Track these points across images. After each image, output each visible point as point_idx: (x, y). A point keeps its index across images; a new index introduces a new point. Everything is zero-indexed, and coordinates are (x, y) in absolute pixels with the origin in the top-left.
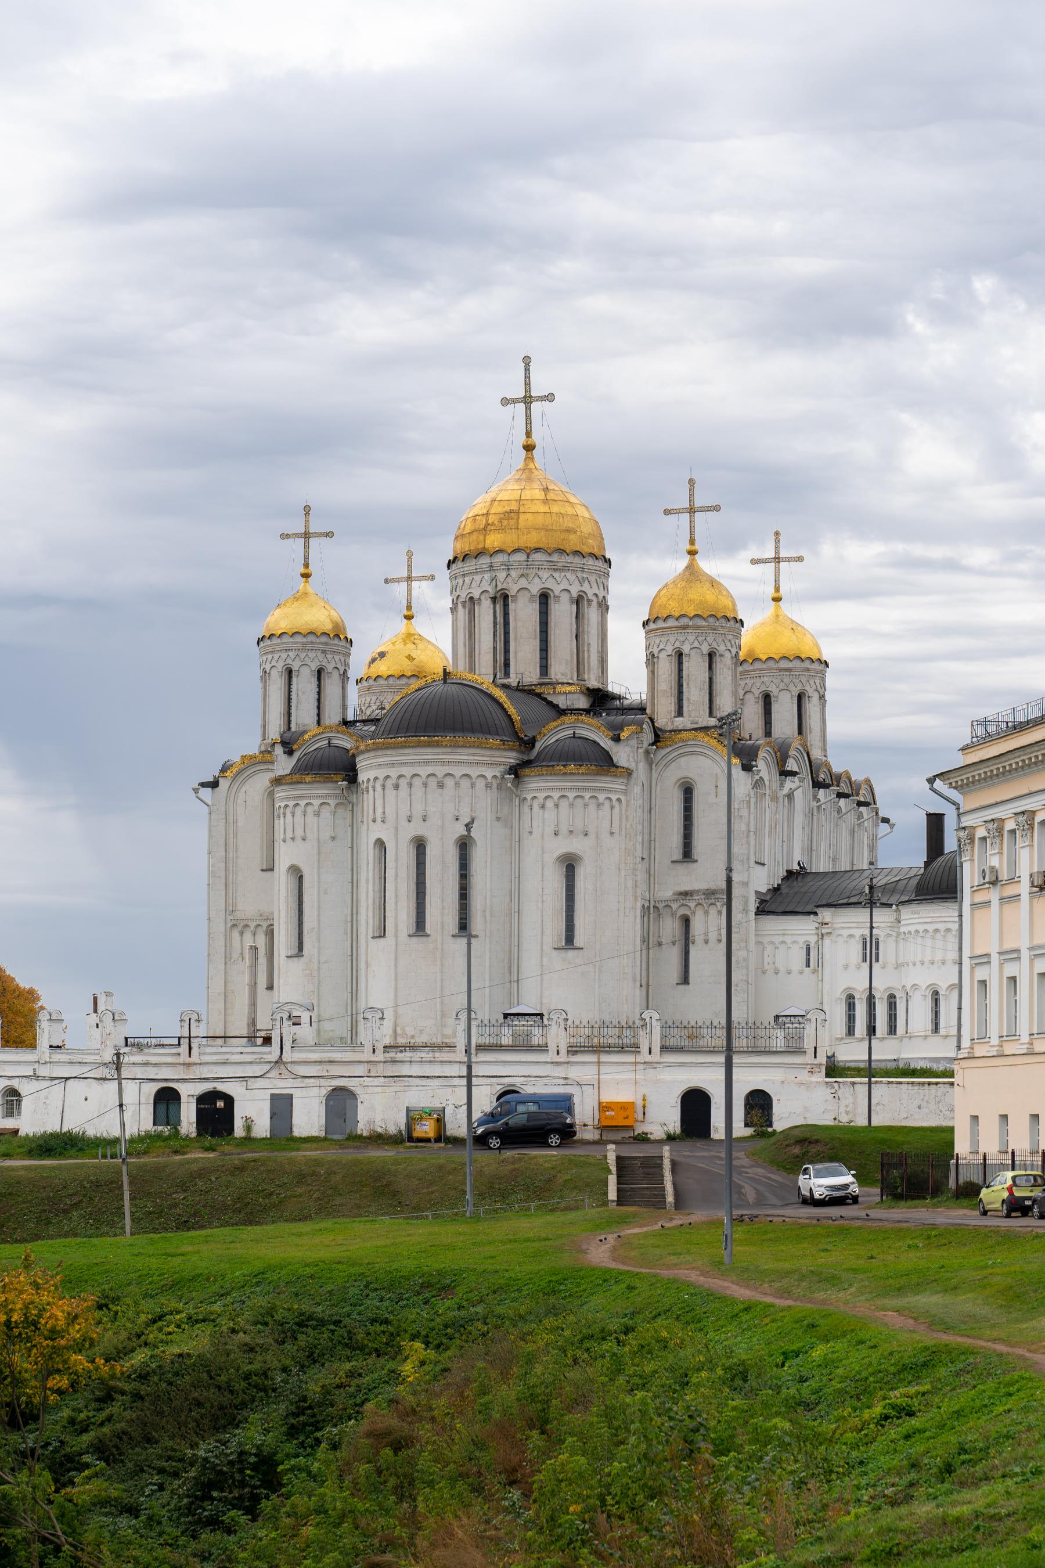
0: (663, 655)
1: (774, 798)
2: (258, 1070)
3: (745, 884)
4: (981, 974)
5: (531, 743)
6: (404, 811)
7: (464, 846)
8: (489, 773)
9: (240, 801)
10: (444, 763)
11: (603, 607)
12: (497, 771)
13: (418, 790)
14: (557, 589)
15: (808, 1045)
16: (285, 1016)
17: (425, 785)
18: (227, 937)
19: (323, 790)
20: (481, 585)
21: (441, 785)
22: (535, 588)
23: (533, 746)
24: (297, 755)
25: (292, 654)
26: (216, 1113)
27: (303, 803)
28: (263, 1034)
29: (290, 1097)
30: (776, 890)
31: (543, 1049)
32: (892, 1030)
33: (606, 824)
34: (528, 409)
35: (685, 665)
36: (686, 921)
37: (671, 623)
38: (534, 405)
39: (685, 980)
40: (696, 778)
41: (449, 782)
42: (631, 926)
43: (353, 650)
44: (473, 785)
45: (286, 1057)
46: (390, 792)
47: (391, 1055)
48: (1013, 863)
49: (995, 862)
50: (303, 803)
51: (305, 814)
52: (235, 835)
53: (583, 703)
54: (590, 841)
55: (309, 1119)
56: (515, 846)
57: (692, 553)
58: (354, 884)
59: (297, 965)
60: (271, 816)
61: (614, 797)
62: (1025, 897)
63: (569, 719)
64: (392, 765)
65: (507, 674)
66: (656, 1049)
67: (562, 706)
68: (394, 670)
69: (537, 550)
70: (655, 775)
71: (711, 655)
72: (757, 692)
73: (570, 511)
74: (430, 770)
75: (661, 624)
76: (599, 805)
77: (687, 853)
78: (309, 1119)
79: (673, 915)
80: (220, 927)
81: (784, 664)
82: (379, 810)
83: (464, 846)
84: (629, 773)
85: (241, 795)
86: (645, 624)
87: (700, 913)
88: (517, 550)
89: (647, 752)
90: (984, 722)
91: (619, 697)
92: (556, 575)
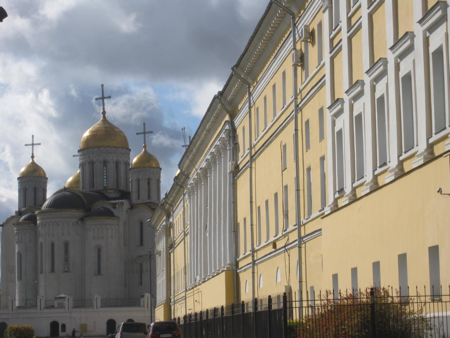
7: (66, 245)
21: (58, 224)
34: (103, 101)
35: (140, 183)
36: (141, 265)
38: (106, 101)
39: (141, 284)
69: (102, 147)
71: (149, 180)
77: (142, 243)
83: (66, 245)
89: (127, 211)
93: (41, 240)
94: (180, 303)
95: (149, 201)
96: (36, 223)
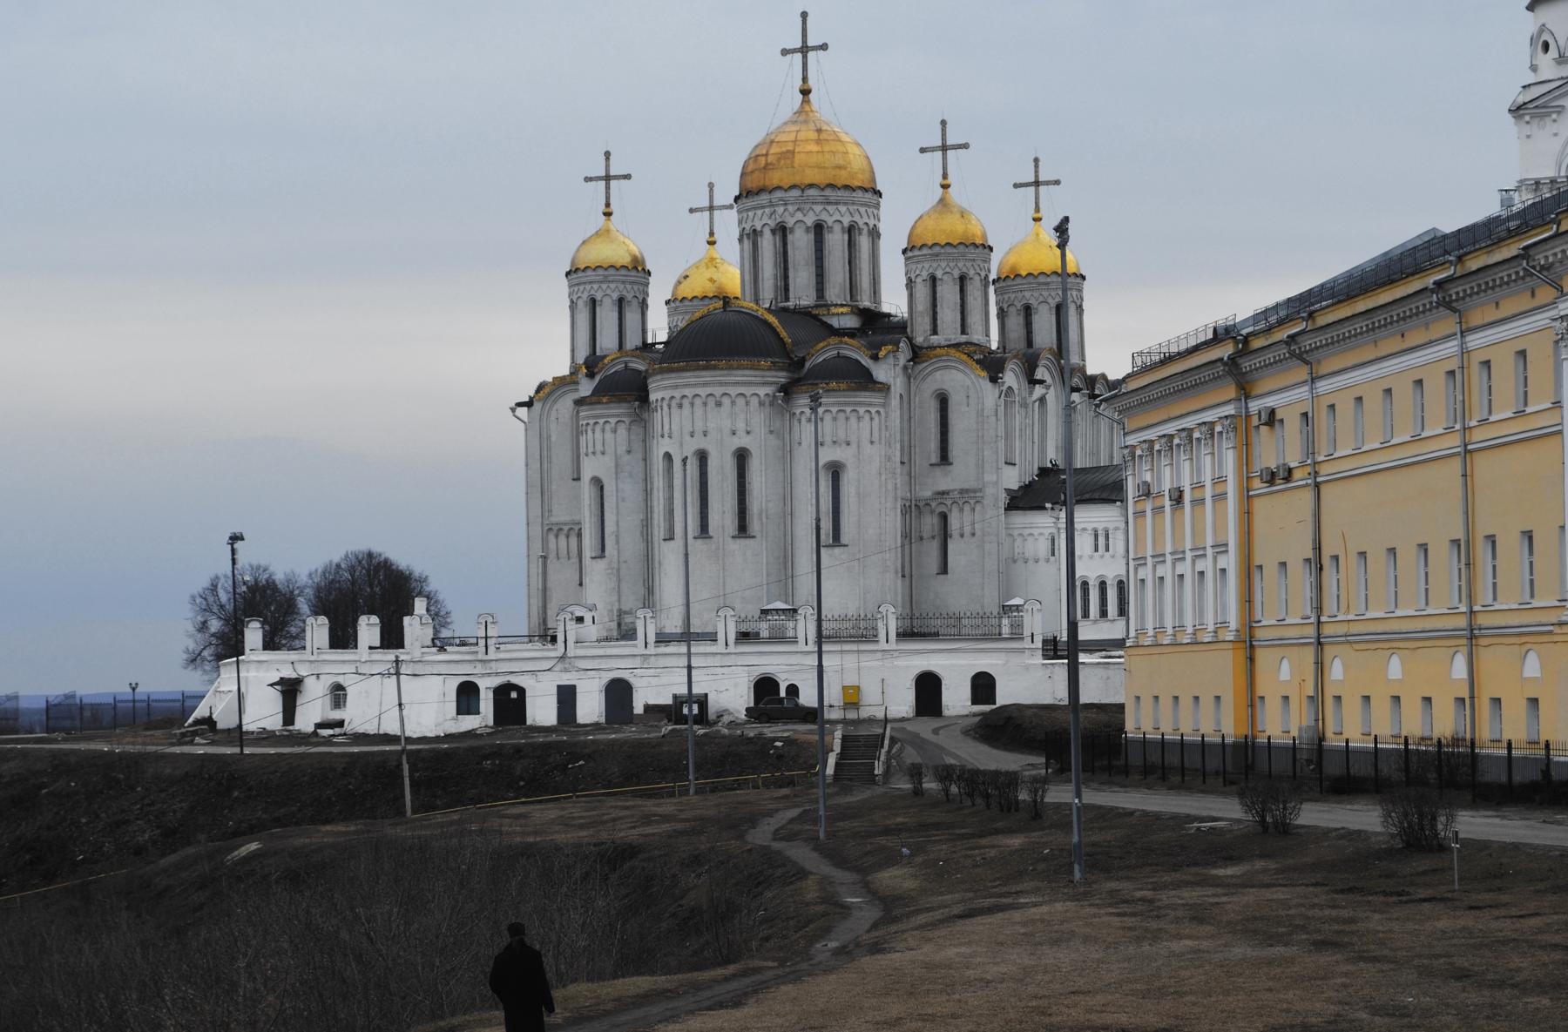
0: (919, 280)
1: (1024, 405)
2: (546, 665)
3: (996, 483)
4: (1141, 575)
5: (803, 361)
6: (688, 428)
7: (742, 457)
8: (762, 391)
9: (553, 418)
10: (721, 384)
11: (875, 234)
12: (769, 390)
13: (699, 411)
14: (830, 221)
15: (1027, 633)
16: (569, 616)
17: (705, 404)
18: (545, 541)
20: (762, 220)
21: (719, 404)
22: (810, 220)
24: (598, 378)
25: (596, 286)
26: (510, 702)
27: (601, 421)
29: (573, 688)
30: (1027, 488)
31: (794, 640)
32: (1123, 611)
33: (866, 435)
34: (805, 58)
35: (939, 289)
36: (944, 518)
37: (925, 251)
38: (811, 55)
39: (944, 570)
41: (726, 401)
42: (892, 523)
43: (651, 279)
44: (747, 403)
45: (570, 653)
46: (675, 410)
47: (663, 649)
48: (1159, 480)
49: (1148, 477)
50: (601, 421)
51: (603, 431)
52: (549, 449)
53: (851, 322)
54: (852, 450)
55: (590, 708)
56: (786, 456)
57: (945, 187)
58: (648, 493)
59: (601, 564)
60: (577, 433)
61: (873, 410)
62: (1168, 509)
63: (833, 340)
64: (676, 387)
65: (787, 299)
67: (836, 325)
68: (698, 292)
71: (963, 279)
72: (1019, 305)
73: (841, 149)
74: (709, 390)
75: (916, 253)
76: (859, 418)
77: (944, 458)
78: (590, 708)
79: (932, 512)
80: (537, 530)
81: (1042, 279)
82: (666, 427)
83: (742, 457)
84: (885, 388)
85: (554, 413)
86: (904, 252)
87: (955, 509)
88: (793, 187)
89: (905, 368)
91: (889, 315)
92: (829, 208)
93: (661, 447)
94: (1356, 646)
95: (963, 338)
96: (643, 398)
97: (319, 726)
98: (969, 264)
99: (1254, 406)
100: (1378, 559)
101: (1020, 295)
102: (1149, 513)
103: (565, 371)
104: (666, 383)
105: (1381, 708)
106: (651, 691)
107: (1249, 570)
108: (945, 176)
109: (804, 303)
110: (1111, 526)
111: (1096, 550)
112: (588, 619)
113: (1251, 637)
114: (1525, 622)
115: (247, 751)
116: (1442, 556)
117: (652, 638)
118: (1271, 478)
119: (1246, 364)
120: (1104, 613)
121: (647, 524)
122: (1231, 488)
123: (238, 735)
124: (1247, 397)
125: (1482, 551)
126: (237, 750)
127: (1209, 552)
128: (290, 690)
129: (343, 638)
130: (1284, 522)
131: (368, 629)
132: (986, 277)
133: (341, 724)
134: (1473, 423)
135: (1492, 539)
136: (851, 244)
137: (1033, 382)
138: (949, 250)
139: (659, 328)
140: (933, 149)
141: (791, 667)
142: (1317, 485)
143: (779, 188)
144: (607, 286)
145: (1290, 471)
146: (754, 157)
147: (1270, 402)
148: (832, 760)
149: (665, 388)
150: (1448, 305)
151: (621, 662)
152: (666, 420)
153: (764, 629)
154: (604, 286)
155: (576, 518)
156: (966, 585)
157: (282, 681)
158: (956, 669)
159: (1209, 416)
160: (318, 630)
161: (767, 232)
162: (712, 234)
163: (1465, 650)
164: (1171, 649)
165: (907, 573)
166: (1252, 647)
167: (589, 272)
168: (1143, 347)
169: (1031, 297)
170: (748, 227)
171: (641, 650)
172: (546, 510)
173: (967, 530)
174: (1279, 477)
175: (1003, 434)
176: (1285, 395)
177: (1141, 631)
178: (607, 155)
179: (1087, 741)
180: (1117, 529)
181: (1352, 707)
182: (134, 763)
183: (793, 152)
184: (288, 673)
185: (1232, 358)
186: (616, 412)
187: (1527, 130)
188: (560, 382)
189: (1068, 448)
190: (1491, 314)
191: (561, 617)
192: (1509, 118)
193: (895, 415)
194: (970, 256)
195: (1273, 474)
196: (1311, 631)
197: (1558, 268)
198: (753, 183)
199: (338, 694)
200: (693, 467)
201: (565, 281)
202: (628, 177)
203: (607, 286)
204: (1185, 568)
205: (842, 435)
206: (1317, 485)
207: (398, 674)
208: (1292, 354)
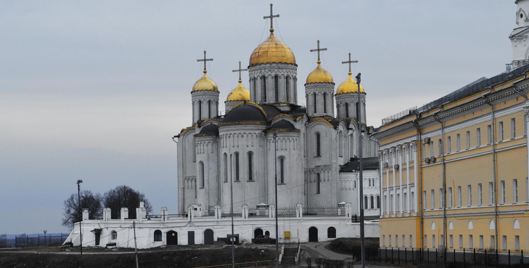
0: (310, 95)
1: (345, 137)
4: (385, 194)
5: (271, 122)
6: (232, 144)
7: (250, 154)
8: (257, 132)
9: (187, 141)
10: (243, 130)
11: (295, 79)
12: (259, 132)
13: (236, 138)
14: (280, 75)
15: (346, 214)
16: (192, 208)
17: (238, 136)
18: (184, 183)
19: (209, 138)
20: (257, 74)
21: (242, 136)
22: (273, 74)
23: (271, 123)
24: (202, 128)
25: (201, 97)
26: (172, 237)
27: (203, 142)
28: (186, 213)
29: (193, 232)
30: (346, 165)
31: (268, 216)
32: (379, 206)
33: (292, 147)
34: (272, 19)
35: (317, 97)
36: (319, 175)
37: (312, 85)
38: (274, 18)
39: (319, 192)
40: (321, 132)
41: (245, 135)
42: (301, 177)
43: (220, 94)
44: (252, 136)
45: (193, 220)
46: (228, 139)
47: (224, 219)
48: (391, 162)
49: (387, 161)
50: (203, 142)
53: (287, 109)
54: (287, 152)
55: (199, 239)
56: (265, 154)
57: (319, 63)
58: (218, 166)
59: (203, 191)
60: (195, 146)
61: (295, 138)
62: (394, 172)
63: (281, 115)
64: (228, 131)
65: (266, 101)
66: (301, 215)
67: (282, 110)
68: (235, 99)
70: (308, 131)
71: (325, 94)
72: (344, 103)
73: (284, 50)
74: (239, 132)
75: (309, 85)
77: (319, 155)
78: (199, 239)
79: (315, 173)
80: (181, 179)
81: (351, 94)
83: (250, 154)
84: (298, 131)
85: (187, 140)
86: (305, 85)
87: (322, 172)
88: (268, 63)
89: (305, 124)
90: (385, 119)
91: (300, 106)
92: (280, 70)
93: (223, 151)
94: (458, 218)
95: (325, 114)
96: (217, 134)
97: (108, 245)
98: (327, 89)
99: (423, 137)
100: (465, 189)
101: (344, 100)
102: (388, 173)
103: (191, 126)
104: (225, 129)
105: (466, 239)
106: (220, 233)
107: (421, 192)
108: (319, 59)
109: (271, 102)
110: (375, 178)
111: (370, 186)
112: (198, 209)
113: (422, 215)
114: (514, 210)
115: (83, 253)
116: (487, 188)
117: (220, 215)
118: (429, 161)
119: (420, 123)
120: (372, 207)
121: (218, 177)
122: (415, 165)
123: (80, 248)
124: (421, 134)
125: (500, 186)
126: (80, 253)
127: (408, 186)
128: (98, 233)
129: (116, 215)
130: (433, 176)
131: (124, 212)
132: (333, 93)
133: (115, 244)
134: (497, 143)
135: (503, 182)
136: (287, 82)
137: (348, 129)
138: (320, 84)
139: (222, 111)
140: (315, 50)
141: (267, 225)
142: (444, 164)
143: (263, 63)
144: (205, 97)
145: (435, 159)
146: (254, 53)
147: (429, 136)
148: (281, 257)
149: (224, 131)
150: (488, 103)
151: (210, 223)
152: (225, 142)
153: (258, 212)
154: (204, 97)
155: (195, 175)
156: (326, 197)
157: (95, 230)
158: (322, 226)
159: (408, 140)
160: (107, 213)
161: (259, 78)
162: (240, 79)
163: (494, 219)
164: (395, 219)
165: (306, 193)
166: (422, 218)
167: (199, 92)
168: (386, 117)
169: (348, 100)
170: (252, 77)
171: (216, 219)
172: (184, 172)
173: (326, 179)
174: (431, 161)
175: (339, 147)
176: (433, 133)
177: (385, 213)
178: (205, 52)
179: (366, 249)
180: (377, 178)
181: (456, 239)
182: (45, 257)
183: (268, 51)
184: (97, 227)
185: (416, 121)
186: (208, 139)
187: (515, 44)
188: (189, 129)
189: (360, 151)
190: (503, 106)
191: (189, 208)
192: (509, 40)
193: (302, 140)
194: (327, 87)
195: (429, 160)
196: (442, 213)
197: (526, 91)
198: (254, 62)
199: (114, 234)
200: (234, 157)
201: (191, 95)
202: (212, 60)
203: (205, 97)
204: (400, 192)
205: (284, 147)
206: (444, 164)
207: (134, 227)
208: (436, 120)
